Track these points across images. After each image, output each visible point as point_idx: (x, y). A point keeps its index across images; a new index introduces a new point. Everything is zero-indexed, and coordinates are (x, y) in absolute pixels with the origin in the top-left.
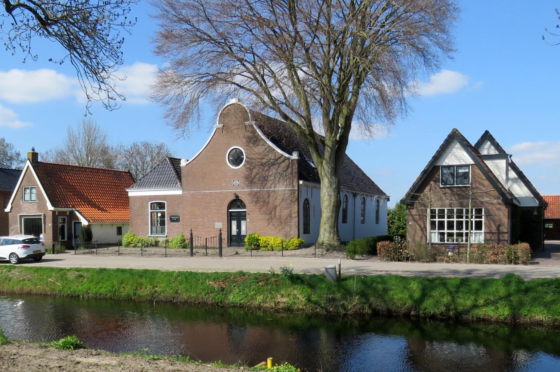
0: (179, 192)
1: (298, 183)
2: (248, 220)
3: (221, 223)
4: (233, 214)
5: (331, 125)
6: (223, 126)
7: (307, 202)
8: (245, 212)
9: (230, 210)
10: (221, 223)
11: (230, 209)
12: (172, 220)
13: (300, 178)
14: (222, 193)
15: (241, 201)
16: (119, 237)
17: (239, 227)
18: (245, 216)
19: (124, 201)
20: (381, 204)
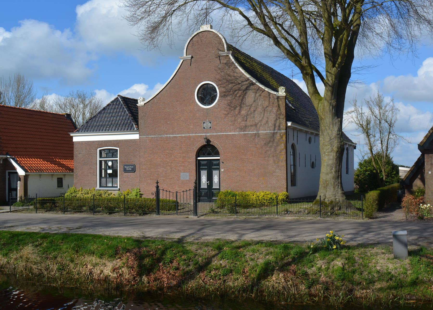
0: (136, 137)
1: (286, 124)
2: (222, 170)
3: (188, 174)
4: (202, 163)
5: (332, 56)
6: (192, 57)
7: (293, 146)
8: (219, 160)
9: (199, 158)
10: (188, 174)
11: (199, 157)
12: (125, 171)
13: (288, 119)
14: (189, 137)
15: (213, 147)
16: (60, 190)
17: (210, 178)
18: (218, 165)
19: (69, 149)
20: (349, 152)
